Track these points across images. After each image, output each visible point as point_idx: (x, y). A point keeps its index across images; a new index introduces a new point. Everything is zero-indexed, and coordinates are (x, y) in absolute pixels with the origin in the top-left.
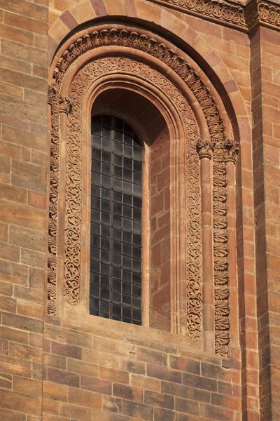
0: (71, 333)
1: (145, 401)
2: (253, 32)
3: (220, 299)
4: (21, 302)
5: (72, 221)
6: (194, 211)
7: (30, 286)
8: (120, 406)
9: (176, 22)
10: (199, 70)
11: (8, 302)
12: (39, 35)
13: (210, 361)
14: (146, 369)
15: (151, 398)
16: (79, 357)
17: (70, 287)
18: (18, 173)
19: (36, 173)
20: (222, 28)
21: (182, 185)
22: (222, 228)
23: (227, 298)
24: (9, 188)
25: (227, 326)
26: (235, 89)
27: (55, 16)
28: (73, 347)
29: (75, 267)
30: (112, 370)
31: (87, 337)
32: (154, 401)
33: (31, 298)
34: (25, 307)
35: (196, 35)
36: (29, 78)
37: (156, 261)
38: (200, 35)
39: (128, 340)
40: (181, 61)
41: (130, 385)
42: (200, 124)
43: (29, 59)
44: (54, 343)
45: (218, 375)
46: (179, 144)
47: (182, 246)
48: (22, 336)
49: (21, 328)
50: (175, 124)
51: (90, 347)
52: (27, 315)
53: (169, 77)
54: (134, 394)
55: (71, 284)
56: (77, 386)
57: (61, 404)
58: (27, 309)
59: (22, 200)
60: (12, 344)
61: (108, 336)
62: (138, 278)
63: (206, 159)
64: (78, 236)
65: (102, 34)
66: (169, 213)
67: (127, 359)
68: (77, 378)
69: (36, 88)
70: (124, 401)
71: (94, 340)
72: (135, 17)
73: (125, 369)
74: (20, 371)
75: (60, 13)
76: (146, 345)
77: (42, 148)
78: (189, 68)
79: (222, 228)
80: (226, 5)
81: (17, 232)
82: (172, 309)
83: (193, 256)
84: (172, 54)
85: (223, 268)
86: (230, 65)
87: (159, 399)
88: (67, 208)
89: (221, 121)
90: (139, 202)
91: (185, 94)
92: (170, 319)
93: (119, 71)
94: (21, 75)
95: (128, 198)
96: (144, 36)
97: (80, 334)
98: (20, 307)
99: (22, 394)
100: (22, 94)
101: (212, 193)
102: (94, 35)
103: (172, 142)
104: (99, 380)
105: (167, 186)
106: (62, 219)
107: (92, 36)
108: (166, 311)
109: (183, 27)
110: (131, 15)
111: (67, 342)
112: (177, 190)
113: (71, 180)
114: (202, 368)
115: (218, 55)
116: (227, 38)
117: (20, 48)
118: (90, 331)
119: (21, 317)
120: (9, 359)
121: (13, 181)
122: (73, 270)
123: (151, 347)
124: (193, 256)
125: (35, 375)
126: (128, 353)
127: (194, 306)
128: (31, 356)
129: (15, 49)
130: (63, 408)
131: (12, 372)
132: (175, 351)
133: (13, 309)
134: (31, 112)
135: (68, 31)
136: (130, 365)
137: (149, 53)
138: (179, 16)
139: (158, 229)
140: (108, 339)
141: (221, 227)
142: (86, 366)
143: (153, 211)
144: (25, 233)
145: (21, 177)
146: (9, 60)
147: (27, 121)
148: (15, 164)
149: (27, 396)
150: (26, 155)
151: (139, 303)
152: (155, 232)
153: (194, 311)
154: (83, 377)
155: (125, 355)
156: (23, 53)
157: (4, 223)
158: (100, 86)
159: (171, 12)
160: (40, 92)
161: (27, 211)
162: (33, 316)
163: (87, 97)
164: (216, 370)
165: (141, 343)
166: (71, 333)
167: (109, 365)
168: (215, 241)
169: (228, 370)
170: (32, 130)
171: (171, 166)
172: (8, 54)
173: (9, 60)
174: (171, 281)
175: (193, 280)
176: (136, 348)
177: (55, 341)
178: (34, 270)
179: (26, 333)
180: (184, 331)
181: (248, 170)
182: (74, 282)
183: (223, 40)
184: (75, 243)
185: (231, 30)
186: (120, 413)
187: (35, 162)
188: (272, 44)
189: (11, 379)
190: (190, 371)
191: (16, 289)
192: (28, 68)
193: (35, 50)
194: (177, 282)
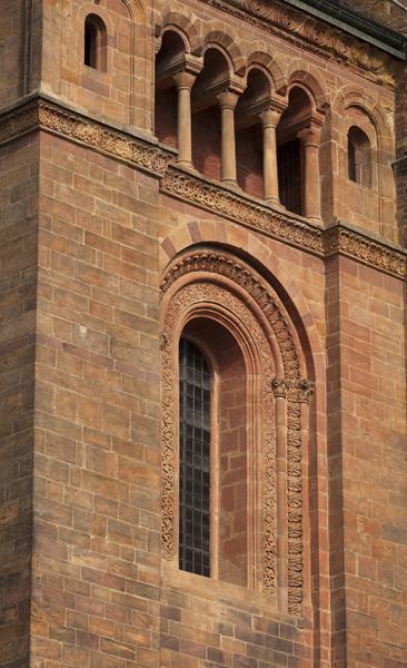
2: (330, 259)
4: (141, 567)
6: (269, 456)
9: (261, 247)
10: (278, 300)
16: (178, 619)
21: (259, 427)
23: (300, 552)
24: (128, 444)
26: (311, 324)
28: (174, 609)
31: (185, 598)
35: (278, 262)
36: (144, 321)
37: (227, 503)
38: (282, 261)
41: (221, 648)
42: (275, 359)
46: (256, 381)
47: (260, 494)
53: (249, 306)
54: (225, 658)
55: (166, 537)
56: (177, 650)
59: (140, 458)
62: (207, 520)
66: (246, 457)
67: (218, 621)
69: (149, 332)
77: (157, 400)
78: (269, 297)
81: (137, 492)
84: (254, 282)
89: (296, 357)
90: (207, 435)
92: (246, 572)
95: (198, 431)
103: (249, 377)
105: (242, 426)
109: (267, 253)
118: (188, 591)
122: (168, 522)
125: (154, 646)
126: (219, 614)
132: (257, 611)
133: (133, 575)
136: (221, 626)
138: (262, 240)
139: (230, 470)
143: (222, 450)
144: (144, 493)
147: (142, 369)
148: (134, 416)
150: (142, 405)
151: (207, 548)
156: (138, 293)
165: (229, 604)
170: (148, 379)
172: (126, 294)
173: (127, 301)
180: (261, 586)
181: (322, 414)
183: (301, 267)
185: (309, 256)
191: (137, 554)
194: (253, 533)
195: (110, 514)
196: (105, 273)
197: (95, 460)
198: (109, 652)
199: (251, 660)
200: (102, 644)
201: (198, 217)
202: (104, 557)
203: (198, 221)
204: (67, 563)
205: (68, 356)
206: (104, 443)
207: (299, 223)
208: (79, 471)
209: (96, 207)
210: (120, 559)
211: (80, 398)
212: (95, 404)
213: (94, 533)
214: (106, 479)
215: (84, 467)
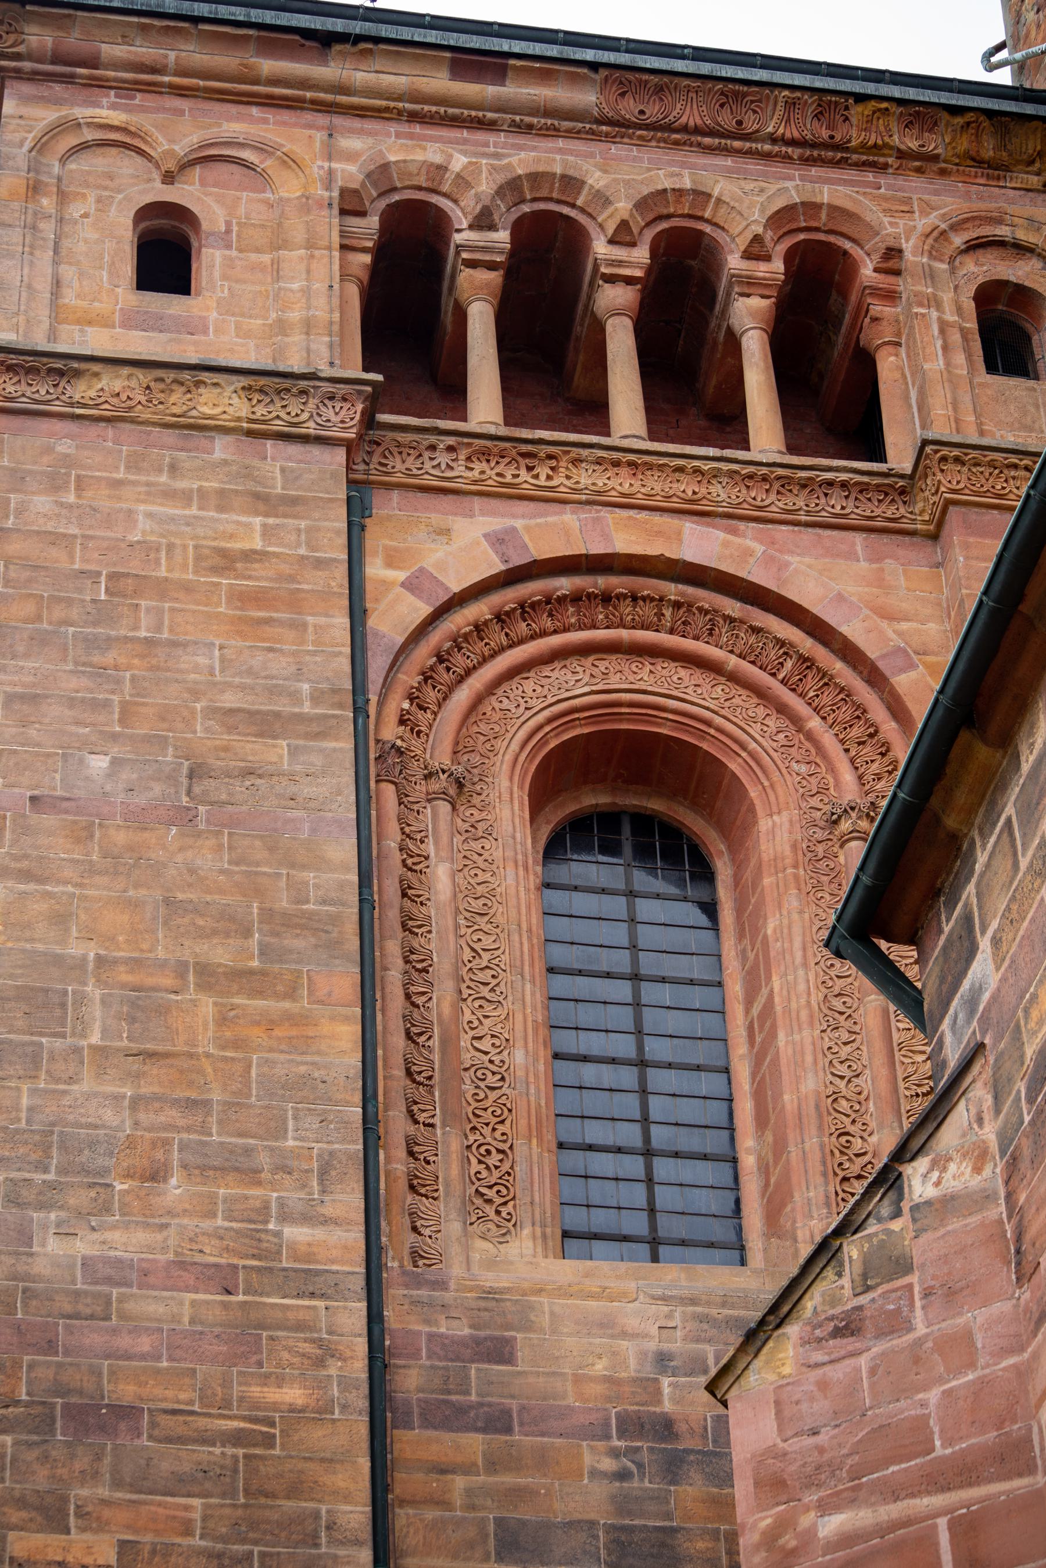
0: (482, 1304)
1: (715, 1441)
4: (296, 1233)
5: (485, 1045)
7: (323, 1192)
8: (640, 1466)
10: (806, 644)
11: (260, 1240)
12: (322, 620)
16: (508, 1359)
17: (489, 1201)
18: (278, 935)
19: (329, 928)
20: (858, 540)
24: (251, 972)
27: (386, 585)
28: (492, 1338)
29: (499, 1151)
30: (608, 1380)
33: (325, 1221)
34: (309, 1245)
36: (300, 718)
39: (653, 1298)
40: (756, 630)
41: (667, 1406)
43: (299, 674)
44: (431, 1336)
48: (301, 1315)
49: (298, 1296)
50: (766, 783)
51: (542, 1330)
52: (317, 1262)
53: (734, 678)
54: (682, 1427)
55: (491, 1193)
56: (508, 1430)
57: (460, 1482)
58: (315, 1250)
59: (291, 994)
60: (271, 1338)
61: (591, 1296)
64: (503, 1079)
65: (526, 609)
67: (652, 1346)
68: (507, 1413)
71: (552, 1313)
72: (609, 551)
73: (649, 1371)
74: (300, 1402)
75: (401, 576)
76: (708, 1304)
78: (781, 643)
80: (857, 483)
82: (799, 1218)
83: (842, 1077)
86: (890, 616)
88: (468, 1016)
91: (782, 709)
93: (594, 688)
94: (277, 715)
96: (646, 593)
97: (508, 1304)
98: (292, 1247)
99: (306, 1459)
100: (281, 757)
102: (508, 614)
106: (449, 1043)
107: (501, 618)
109: (749, 553)
110: (597, 548)
111: (471, 1327)
113: (473, 950)
115: (854, 599)
116: (876, 558)
117: (271, 655)
118: (540, 1291)
119: (295, 1270)
120: (267, 1376)
121: (262, 953)
123: (724, 1305)
124: (842, 1077)
125: (344, 1407)
126: (654, 1330)
128: (330, 1361)
129: (257, 660)
130: (469, 1492)
131: (275, 1407)
134: (307, 790)
135: (425, 610)
137: (671, 632)
138: (734, 532)
140: (593, 1304)
142: (531, 1380)
144: (303, 1069)
145: (286, 942)
146: (242, 687)
148: (268, 915)
149: (322, 1460)
154: (523, 1409)
155: (646, 1336)
156: (280, 666)
157: (239, 1055)
158: (547, 729)
159: (708, 525)
160: (333, 744)
161: (307, 1017)
162: (333, 1262)
163: (509, 757)
165: (693, 1301)
166: (482, 1304)
167: (600, 1367)
173: (242, 687)
175: (847, 1134)
176: (677, 1314)
177: (434, 1329)
178: (331, 1154)
182: (496, 1188)
183: (864, 564)
184: (493, 1095)
186: (642, 1480)
187: (324, 902)
189: (272, 1424)
192: (295, 697)
193: (314, 653)
195: (188, 1129)
196: (174, 644)
197: (132, 1020)
198: (181, 1440)
200: (153, 1425)
201: (514, 516)
202: (166, 1226)
203: (519, 524)
204: (32, 1255)
205: (48, 820)
206: (168, 981)
208: (77, 1050)
209: (143, 523)
210: (220, 1222)
211: (84, 898)
212: (136, 905)
213: (128, 1175)
214: (167, 1055)
215: (95, 1039)
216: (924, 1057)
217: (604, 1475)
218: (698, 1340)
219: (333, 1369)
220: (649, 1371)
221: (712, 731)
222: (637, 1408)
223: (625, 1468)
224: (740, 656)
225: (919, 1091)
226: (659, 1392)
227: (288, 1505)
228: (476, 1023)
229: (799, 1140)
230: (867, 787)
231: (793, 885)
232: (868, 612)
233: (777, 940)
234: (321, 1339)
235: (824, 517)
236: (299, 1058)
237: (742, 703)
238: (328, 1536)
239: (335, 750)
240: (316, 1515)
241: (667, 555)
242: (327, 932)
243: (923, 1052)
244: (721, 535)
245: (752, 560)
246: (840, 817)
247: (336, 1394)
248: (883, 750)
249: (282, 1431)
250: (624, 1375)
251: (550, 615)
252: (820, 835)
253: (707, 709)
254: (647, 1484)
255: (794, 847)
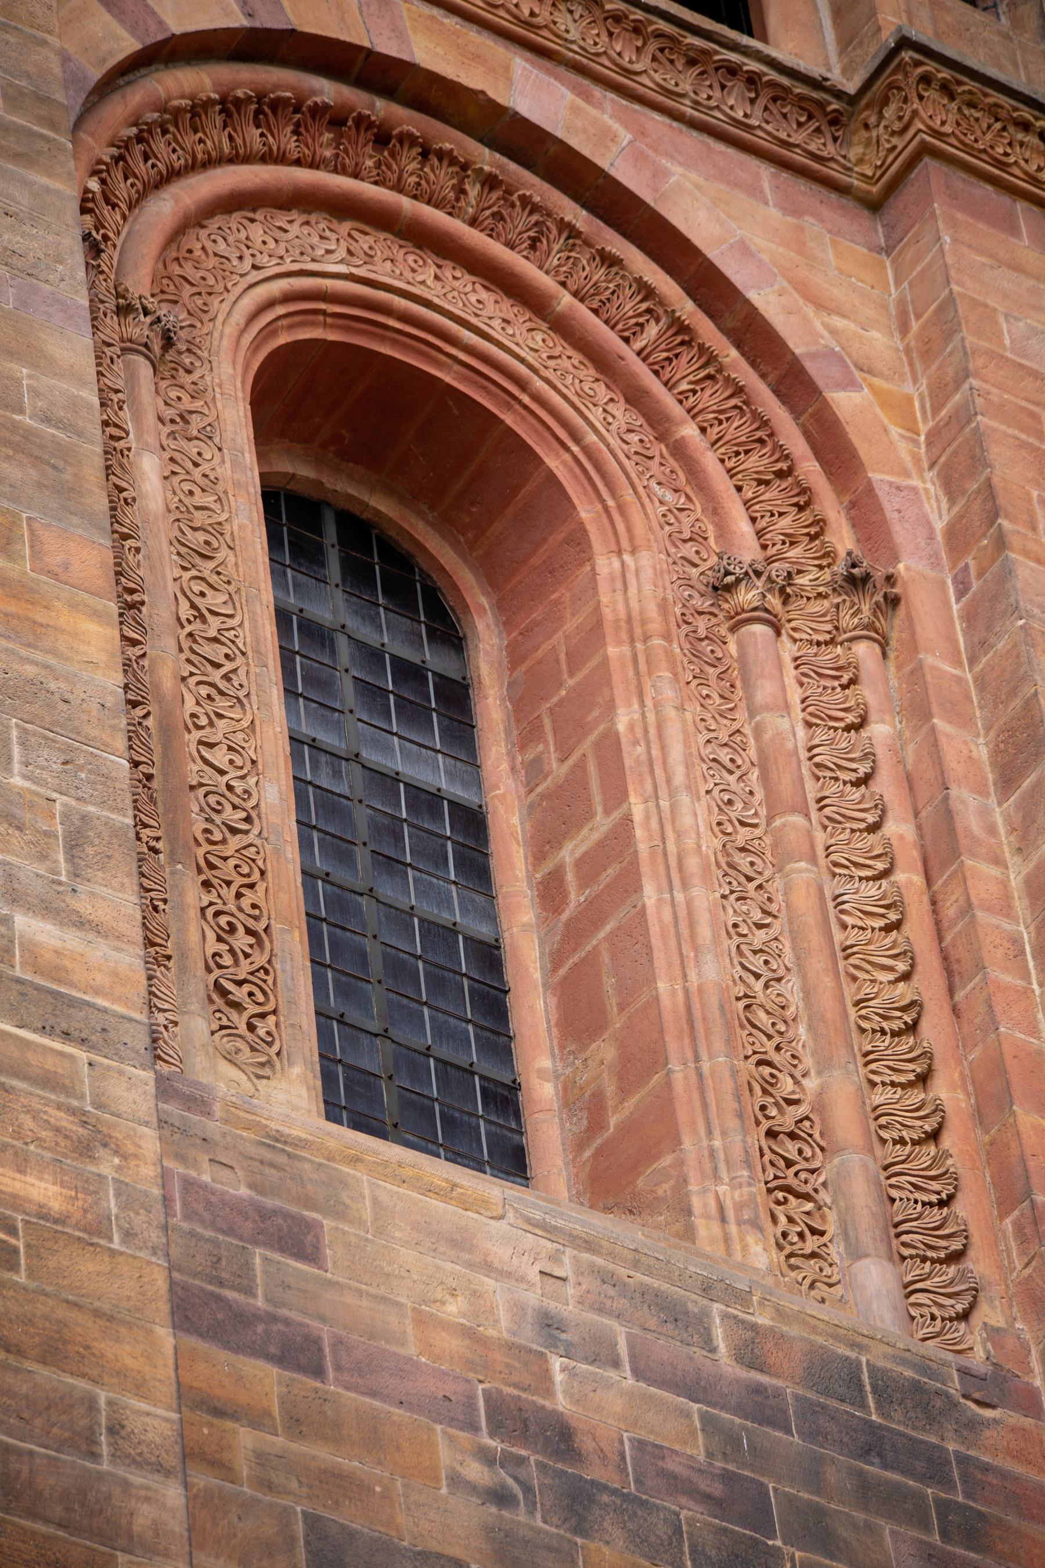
0: (267, 1155)
1: (638, 1481)
3: (902, 1141)
5: (220, 757)
8: (527, 1489)
13: (904, 1362)
14: (623, 1350)
15: (663, 1473)
17: (237, 1006)
19: (61, 464)
20: (765, 174)
21: (670, 712)
22: (868, 879)
23: (934, 1136)
25: (956, 1245)
29: (249, 932)
30: (469, 1334)
32: (677, 1485)
33: (81, 923)
35: (665, 173)
38: (676, 172)
39: (529, 1221)
40: (610, 261)
41: (561, 1403)
45: (950, 1426)
48: (50, 1063)
50: (611, 503)
51: (360, 1223)
52: (71, 984)
54: (587, 1445)
55: (239, 994)
58: (67, 963)
63: (758, 628)
64: (248, 820)
66: (628, 819)
67: (532, 1298)
68: (313, 1343)
70: (542, 1467)
71: (376, 1201)
73: (529, 1337)
74: (56, 1206)
76: (612, 1255)
79: (868, 879)
80: (772, 84)
82: (693, 1176)
83: (757, 976)
85: (896, 1025)
87: (704, 1485)
88: (190, 705)
92: (688, 1212)
96: (447, 146)
98: (30, 948)
101: (804, 755)
102: (238, 103)
103: (605, 565)
104: (417, 1365)
108: (665, 1189)
111: (251, 1186)
112: (653, 732)
113: (193, 606)
114: (875, 1391)
115: (765, 257)
119: (38, 988)
122: (241, 941)
123: (636, 1265)
124: (757, 976)
125: (128, 1235)
126: (533, 1274)
127: (789, 1164)
128: (101, 1153)
135: (129, 45)
137: (473, 222)
138: (587, 97)
140: (436, 1204)
141: (863, 873)
142: (350, 1299)
144: (30, 670)
149: (97, 1313)
152: (564, 917)
153: (791, 1181)
154: (338, 1343)
155: (521, 1279)
158: (281, 310)
159: (549, 72)
160: (44, 180)
161: (32, 591)
162: (97, 992)
163: (230, 330)
164: (938, 1403)
166: (267, 1155)
167: (454, 1309)
168: (844, 926)
169: (988, 1413)
171: (612, 651)
174: (675, 1066)
176: (566, 1260)
177: (193, 1174)
179: (71, 1057)
182: (246, 988)
183: (774, 213)
184: (235, 842)
186: (531, 1512)
187: (47, 420)
188: (981, 226)
189: (12, 1231)
190: (826, 1392)
199: (728, 1478)
207: (734, 57)
216: (891, 977)
217: (472, 1488)
218: (601, 1310)
219: (107, 1166)
220: (529, 1337)
221: (526, 399)
222: (516, 1392)
223: (504, 1486)
224: (575, 294)
225: (885, 1025)
226: (546, 1375)
227: (44, 1373)
228: (203, 721)
229: (689, 1054)
230: (771, 551)
231: (663, 664)
232: (785, 284)
233: (636, 743)
234: (84, 1113)
235: (716, 119)
236: (23, 652)
237: (571, 369)
238: (113, 1445)
239: (48, 190)
240: (91, 1405)
241: (491, 94)
242: (55, 467)
243: (891, 969)
244: (569, 96)
245: (615, 149)
246: (738, 581)
247: (114, 1210)
248: (802, 500)
249: (28, 1246)
250: (491, 1332)
251: (296, 132)
252: (705, 604)
253: (522, 361)
254: (540, 1524)
255: (663, 607)
